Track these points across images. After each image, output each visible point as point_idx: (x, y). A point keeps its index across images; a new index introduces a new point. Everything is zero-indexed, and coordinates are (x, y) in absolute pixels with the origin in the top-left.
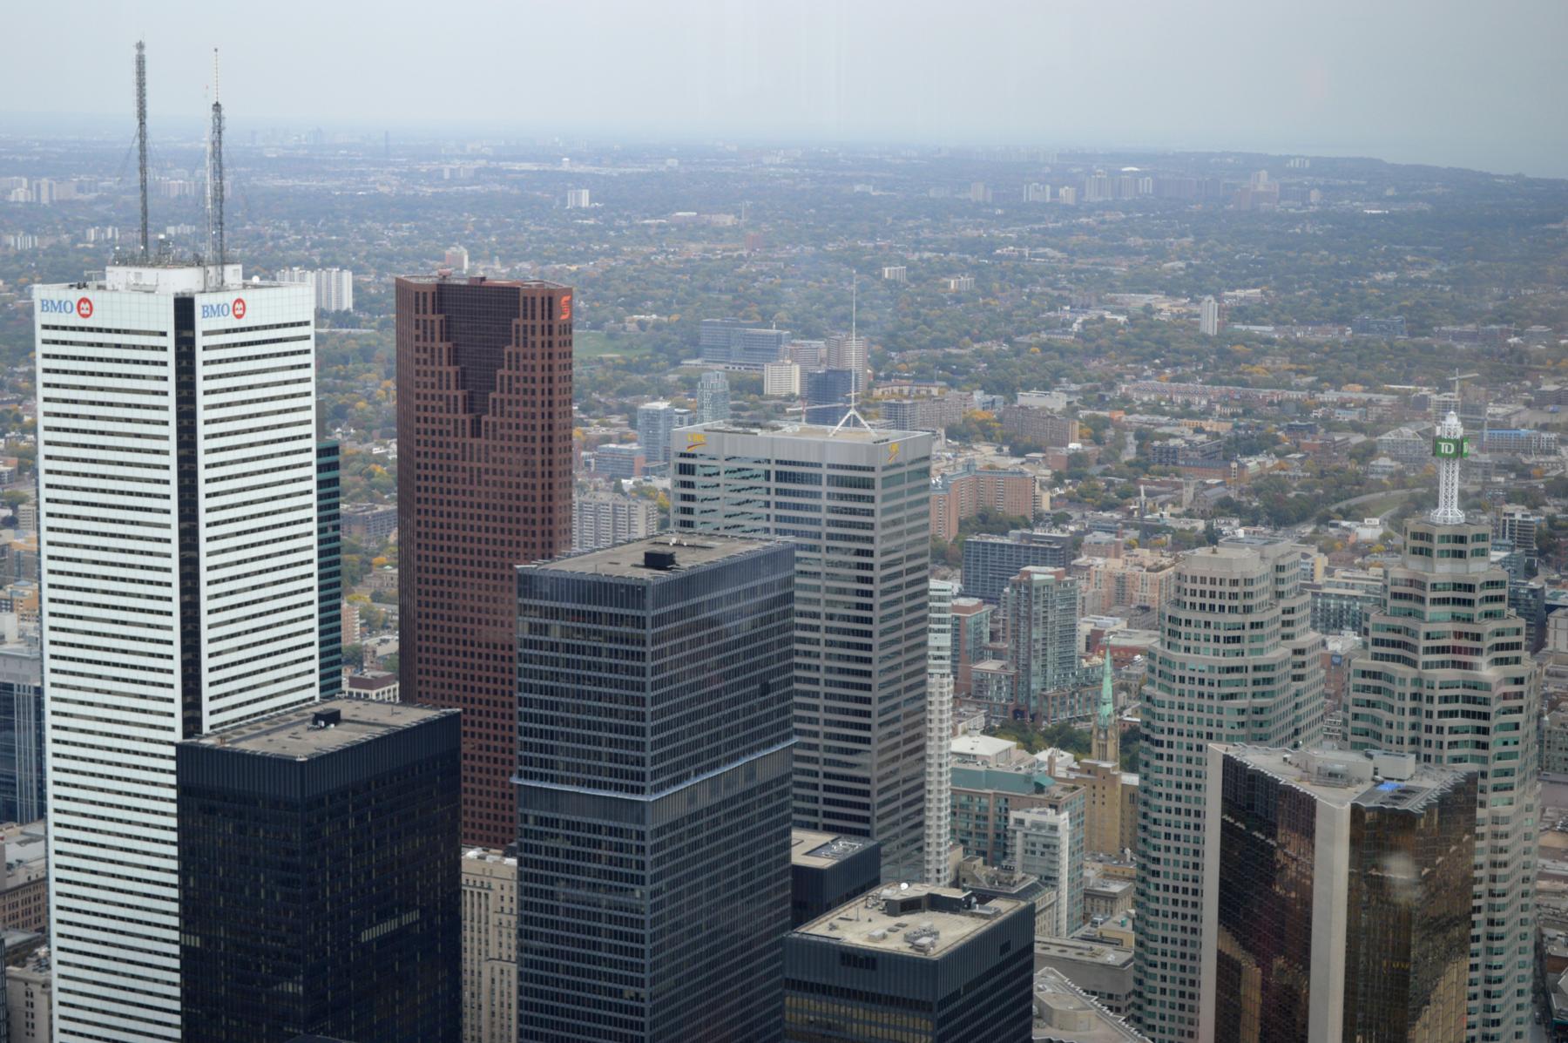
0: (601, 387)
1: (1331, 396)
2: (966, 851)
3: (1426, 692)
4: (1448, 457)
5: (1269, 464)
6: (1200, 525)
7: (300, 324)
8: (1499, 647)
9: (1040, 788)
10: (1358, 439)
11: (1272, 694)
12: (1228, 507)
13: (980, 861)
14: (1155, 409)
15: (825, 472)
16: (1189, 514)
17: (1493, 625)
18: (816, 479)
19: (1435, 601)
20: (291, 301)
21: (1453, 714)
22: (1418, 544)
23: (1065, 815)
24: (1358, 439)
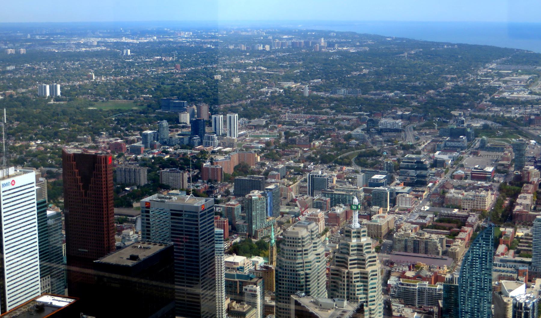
0: (132, 121)
1: (340, 116)
2: (231, 299)
3: (350, 276)
4: (355, 210)
5: (322, 143)
6: (302, 165)
7: (31, 184)
8: (370, 262)
9: (251, 279)
10: (347, 132)
11: (310, 269)
12: (310, 159)
13: (235, 302)
14: (291, 123)
15: (184, 213)
16: (299, 161)
17: (367, 256)
18: (180, 215)
19: (352, 250)
20: (28, 178)
21: (358, 282)
22: (347, 234)
23: (259, 287)
24: (347, 132)
